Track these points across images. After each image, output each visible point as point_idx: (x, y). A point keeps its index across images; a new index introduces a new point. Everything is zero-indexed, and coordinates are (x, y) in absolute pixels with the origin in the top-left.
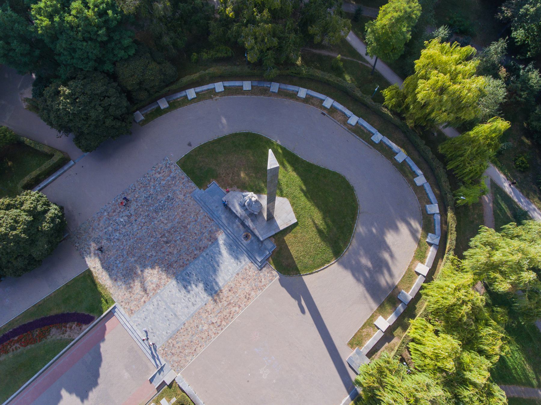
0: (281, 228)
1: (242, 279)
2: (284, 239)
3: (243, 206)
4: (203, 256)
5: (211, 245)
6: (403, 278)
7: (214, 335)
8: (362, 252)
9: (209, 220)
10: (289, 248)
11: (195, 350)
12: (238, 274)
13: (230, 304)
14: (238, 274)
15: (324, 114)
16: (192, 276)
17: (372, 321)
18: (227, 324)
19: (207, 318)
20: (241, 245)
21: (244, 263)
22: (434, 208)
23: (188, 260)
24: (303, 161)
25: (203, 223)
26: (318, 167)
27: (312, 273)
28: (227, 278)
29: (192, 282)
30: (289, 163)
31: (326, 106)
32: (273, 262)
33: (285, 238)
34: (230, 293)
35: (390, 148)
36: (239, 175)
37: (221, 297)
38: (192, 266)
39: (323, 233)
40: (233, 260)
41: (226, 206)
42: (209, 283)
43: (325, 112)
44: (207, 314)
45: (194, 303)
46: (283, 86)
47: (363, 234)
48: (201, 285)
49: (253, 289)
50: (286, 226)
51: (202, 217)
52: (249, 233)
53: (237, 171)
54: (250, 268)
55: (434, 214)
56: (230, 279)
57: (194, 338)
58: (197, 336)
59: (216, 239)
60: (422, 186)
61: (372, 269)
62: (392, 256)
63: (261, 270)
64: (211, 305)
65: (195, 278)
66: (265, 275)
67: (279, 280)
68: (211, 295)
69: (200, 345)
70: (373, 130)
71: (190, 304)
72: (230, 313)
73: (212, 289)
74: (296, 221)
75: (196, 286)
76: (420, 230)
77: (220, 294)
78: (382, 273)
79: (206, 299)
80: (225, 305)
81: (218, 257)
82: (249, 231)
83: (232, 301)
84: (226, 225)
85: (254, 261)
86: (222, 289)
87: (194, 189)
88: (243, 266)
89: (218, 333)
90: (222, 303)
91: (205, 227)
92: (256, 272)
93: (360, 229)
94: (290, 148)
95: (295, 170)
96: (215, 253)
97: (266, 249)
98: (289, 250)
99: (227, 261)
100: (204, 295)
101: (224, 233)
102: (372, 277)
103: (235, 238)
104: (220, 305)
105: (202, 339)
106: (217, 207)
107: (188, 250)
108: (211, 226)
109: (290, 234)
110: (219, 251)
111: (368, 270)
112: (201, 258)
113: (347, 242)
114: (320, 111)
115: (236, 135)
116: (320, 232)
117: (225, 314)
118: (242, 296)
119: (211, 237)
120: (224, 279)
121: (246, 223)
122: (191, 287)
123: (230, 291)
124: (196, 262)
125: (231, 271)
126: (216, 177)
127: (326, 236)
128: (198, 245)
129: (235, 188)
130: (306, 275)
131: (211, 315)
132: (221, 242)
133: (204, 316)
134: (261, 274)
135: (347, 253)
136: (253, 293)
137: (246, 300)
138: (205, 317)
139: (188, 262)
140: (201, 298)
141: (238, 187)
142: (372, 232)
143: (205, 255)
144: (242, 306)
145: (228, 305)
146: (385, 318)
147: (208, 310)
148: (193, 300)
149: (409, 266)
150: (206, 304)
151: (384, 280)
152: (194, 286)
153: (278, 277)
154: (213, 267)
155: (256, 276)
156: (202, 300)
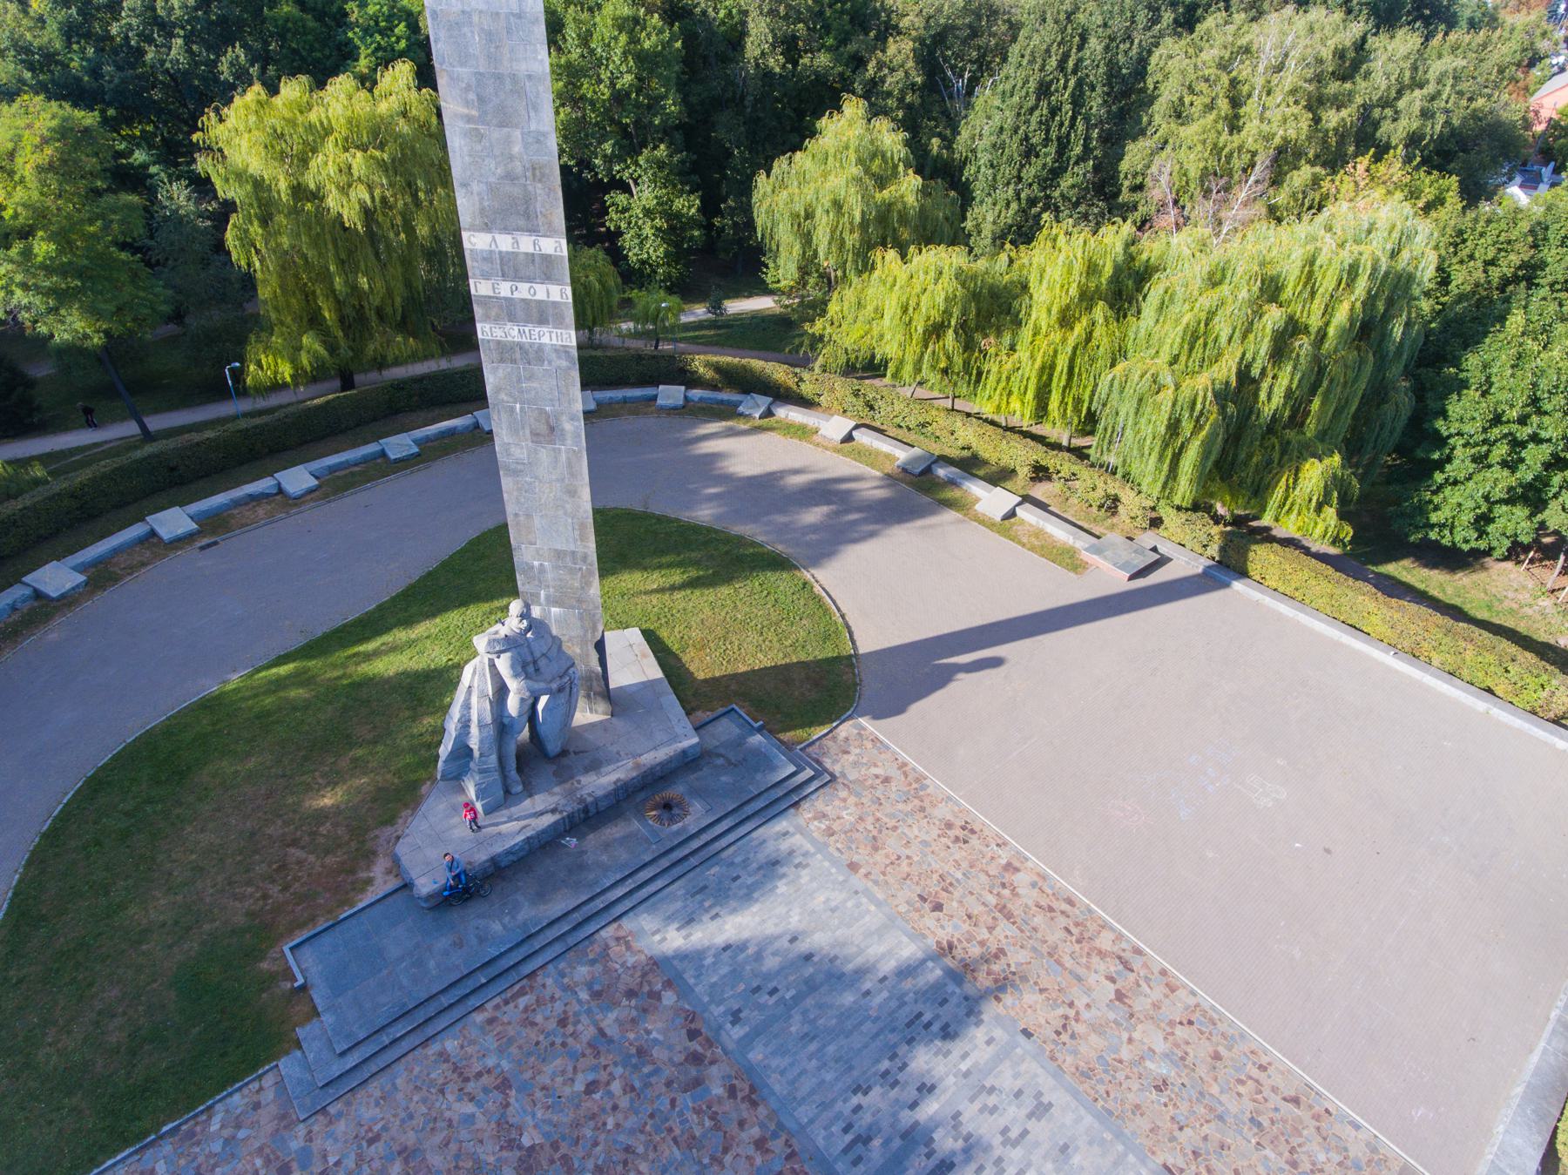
0: (655, 672)
1: (876, 849)
2: (706, 681)
4: (747, 1042)
5: (685, 992)
7: (1181, 993)
8: (781, 519)
9: (523, 1001)
10: (742, 669)
11: (1296, 1101)
12: (853, 867)
13: (1002, 909)
14: (853, 867)
15: (215, 543)
16: (866, 1118)
17: (994, 525)
18: (1104, 926)
19: (1098, 1028)
20: (705, 837)
21: (797, 840)
22: (671, 394)
23: (760, 1144)
24: (380, 608)
25: (533, 1035)
26: (430, 574)
27: (848, 627)
28: (873, 917)
29: (907, 1118)
30: (367, 639)
31: (180, 531)
32: (802, 727)
33: (701, 676)
34: (951, 906)
35: (451, 432)
36: (322, 815)
37: (975, 951)
38: (804, 1113)
39: (698, 578)
40: (782, 887)
41: (467, 889)
42: (904, 1015)
43: (205, 541)
44: (1079, 1028)
45: (1029, 1103)
47: (721, 510)
48: (924, 1060)
49: (922, 809)
51: (490, 1042)
52: (652, 791)
53: (286, 824)
54: (824, 816)
56: (878, 904)
57: (1232, 1105)
58: (1215, 1090)
59: (657, 963)
60: (599, 404)
61: (833, 507)
62: (797, 472)
63: (833, 778)
64: (1024, 1006)
65: (876, 1098)
66: (855, 764)
67: (877, 716)
68: (971, 1008)
69: (1255, 1072)
70: (371, 448)
71: (1038, 1129)
72: (1051, 909)
73: (937, 996)
74: (634, 635)
75: (926, 1089)
76: (724, 423)
77: (959, 953)
78: (849, 492)
79: (998, 1033)
80: (1011, 930)
81: (758, 956)
82: (642, 795)
83: (992, 900)
84: (584, 898)
85: (788, 798)
86: (931, 942)
87: (269, 1095)
88: (813, 841)
89: (1164, 972)
90: (1004, 944)
91: (563, 1022)
92: (843, 794)
93: (704, 514)
95: (408, 622)
96: (736, 974)
97: (739, 743)
98: (753, 671)
99: (782, 910)
100: (979, 1044)
101: (627, 924)
102: (859, 510)
103: (665, 863)
104: (1017, 957)
105: (1217, 1057)
106: (459, 944)
107: (692, 1142)
108: (566, 988)
109: (685, 658)
110: (726, 948)
111: (837, 513)
112: (756, 1055)
113: (741, 541)
114: (188, 553)
115: (53, 837)
116: (692, 584)
117: (1063, 934)
118: (958, 853)
119: (631, 994)
120: (880, 932)
121: (600, 793)
122: (935, 1124)
123: (938, 907)
124: (777, 1085)
125: (837, 897)
126: (264, 931)
127: (714, 574)
128: (668, 1072)
129: (388, 831)
130: (853, 642)
131: (1080, 1003)
132: (673, 940)
133: (1091, 1046)
134: (853, 775)
135: (780, 548)
136: (942, 812)
137: (974, 841)
138: (1094, 1039)
139: (777, 1145)
140: (998, 1059)
141: (390, 821)
142: (717, 496)
143: (738, 1032)
144: (1004, 856)
145: (1009, 916)
146: (978, 500)
147: (1058, 1024)
148: (1013, 1114)
150: (1027, 1033)
151: (872, 489)
152: (930, 1108)
153: (863, 721)
154: (811, 986)
155: (858, 795)
156: (1004, 1055)
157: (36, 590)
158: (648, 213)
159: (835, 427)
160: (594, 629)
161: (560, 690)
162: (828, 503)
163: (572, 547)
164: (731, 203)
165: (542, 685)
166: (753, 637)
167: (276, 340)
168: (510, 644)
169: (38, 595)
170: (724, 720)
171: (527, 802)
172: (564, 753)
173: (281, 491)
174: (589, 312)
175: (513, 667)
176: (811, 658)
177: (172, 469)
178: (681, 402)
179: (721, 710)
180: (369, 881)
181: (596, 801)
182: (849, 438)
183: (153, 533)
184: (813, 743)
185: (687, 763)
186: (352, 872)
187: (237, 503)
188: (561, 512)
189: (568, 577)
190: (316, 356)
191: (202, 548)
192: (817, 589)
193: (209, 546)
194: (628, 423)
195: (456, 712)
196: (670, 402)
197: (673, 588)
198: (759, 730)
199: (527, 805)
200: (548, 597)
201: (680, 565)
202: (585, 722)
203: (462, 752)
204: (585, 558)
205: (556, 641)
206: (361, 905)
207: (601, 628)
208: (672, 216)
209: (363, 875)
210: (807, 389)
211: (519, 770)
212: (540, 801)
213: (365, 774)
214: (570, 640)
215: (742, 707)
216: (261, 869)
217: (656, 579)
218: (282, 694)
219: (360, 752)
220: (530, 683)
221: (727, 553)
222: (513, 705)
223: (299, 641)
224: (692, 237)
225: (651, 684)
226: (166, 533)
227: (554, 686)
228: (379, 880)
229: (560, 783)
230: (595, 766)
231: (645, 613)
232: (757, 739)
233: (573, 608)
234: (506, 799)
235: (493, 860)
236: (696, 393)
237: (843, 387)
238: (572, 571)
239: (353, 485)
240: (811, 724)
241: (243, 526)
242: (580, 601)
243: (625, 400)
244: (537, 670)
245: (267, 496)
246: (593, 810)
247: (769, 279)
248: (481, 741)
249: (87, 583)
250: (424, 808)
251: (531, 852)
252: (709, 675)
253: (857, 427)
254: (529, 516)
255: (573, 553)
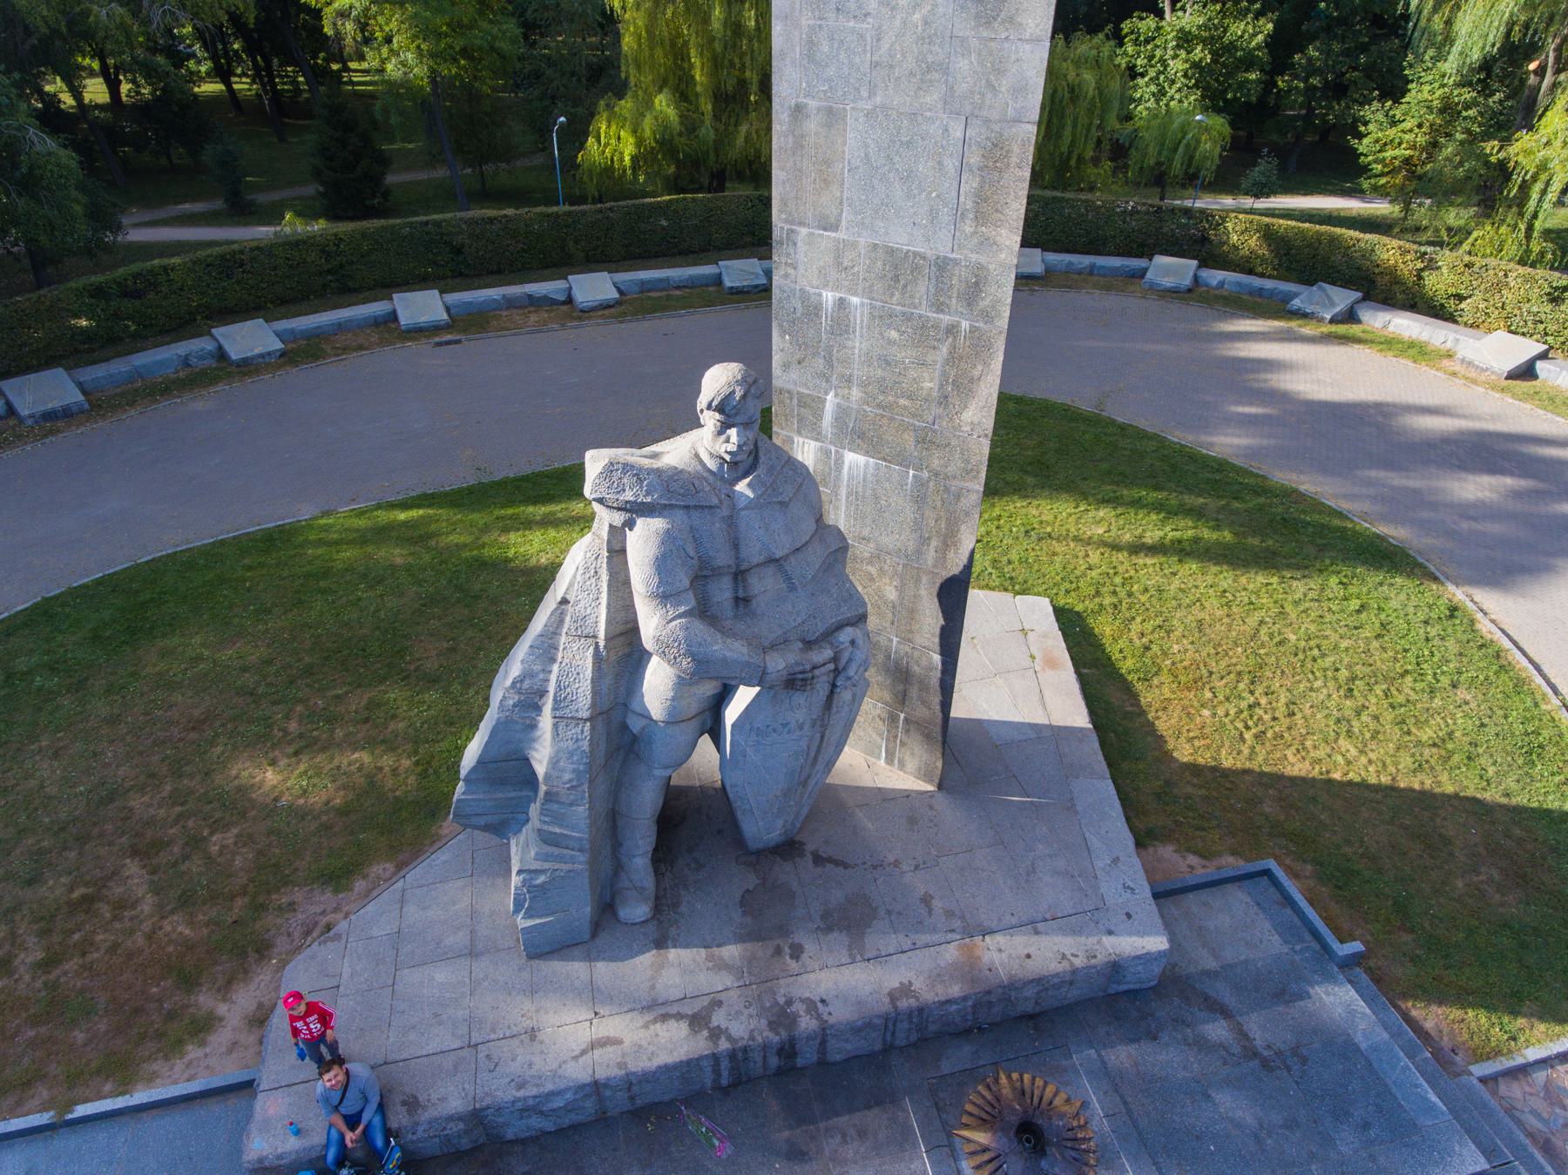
0: (1072, 712)
2: (1194, 769)
3: (588, 927)
6: (1558, 415)
10: (1296, 767)
22: (1170, 269)
33: (1183, 753)
43: (449, 337)
46: (96, 373)
50: (1066, 676)
55: (1196, 277)
74: (1037, 611)
82: (956, 1059)
94: (461, 477)
109: (1148, 697)
121: (840, 1014)
149: (1474, 382)
157: (220, 348)
158: (1185, 40)
159: (1503, 350)
160: (949, 540)
161: (795, 682)
162: (1492, 470)
163: (942, 246)
164: (1313, 52)
165: (736, 650)
166: (1327, 694)
167: (626, 105)
168: (674, 496)
169: (221, 354)
170: (1238, 900)
171: (647, 959)
172: (788, 848)
173: (570, 300)
174: (1067, 132)
175: (662, 565)
176: (1492, 795)
177: (459, 251)
178: (1187, 282)
179: (1232, 864)
180: (202, 1027)
181: (824, 1035)
182: (1526, 372)
183: (393, 317)
184: (1524, 1070)
185: (1116, 1003)
186: (189, 982)
187: (510, 303)
188: (932, 97)
189: (906, 355)
190: (664, 126)
191: (439, 344)
192: (1484, 626)
193: (449, 343)
194: (1093, 300)
195: (514, 666)
196: (1168, 282)
197: (1137, 548)
198: (1348, 963)
199: (645, 969)
200: (842, 415)
201: (1158, 507)
202: (867, 781)
203: (509, 768)
204: (974, 290)
205: (838, 550)
206: (140, 1097)
207: (967, 542)
208: (1222, 50)
209: (204, 1000)
210: (1438, 283)
211: (663, 855)
212: (681, 969)
213: (370, 744)
214: (876, 557)
215: (1294, 875)
216: (54, 889)
217: (1100, 521)
218: (370, 549)
219: (395, 694)
220: (699, 626)
221: (1261, 508)
222: (657, 685)
223: (470, 479)
224: (1242, 85)
225: (1056, 735)
226: (405, 319)
227: (778, 664)
228: (220, 1039)
229: (740, 939)
230: (852, 922)
231: (1067, 574)
232: (1340, 1001)
233: (903, 460)
234: (596, 928)
235: (475, 1116)
236: (1214, 276)
237: (1527, 286)
238: (923, 334)
239: (664, 309)
240: (1511, 1001)
241: (502, 329)
242: (926, 440)
243: (1092, 270)
244: (742, 601)
245: (553, 302)
246: (808, 1056)
247: (1363, 146)
248: (554, 762)
249: (283, 354)
250: (414, 874)
251: (603, 1121)
252: (1204, 759)
253: (1543, 356)
254: (832, 117)
255: (942, 266)
